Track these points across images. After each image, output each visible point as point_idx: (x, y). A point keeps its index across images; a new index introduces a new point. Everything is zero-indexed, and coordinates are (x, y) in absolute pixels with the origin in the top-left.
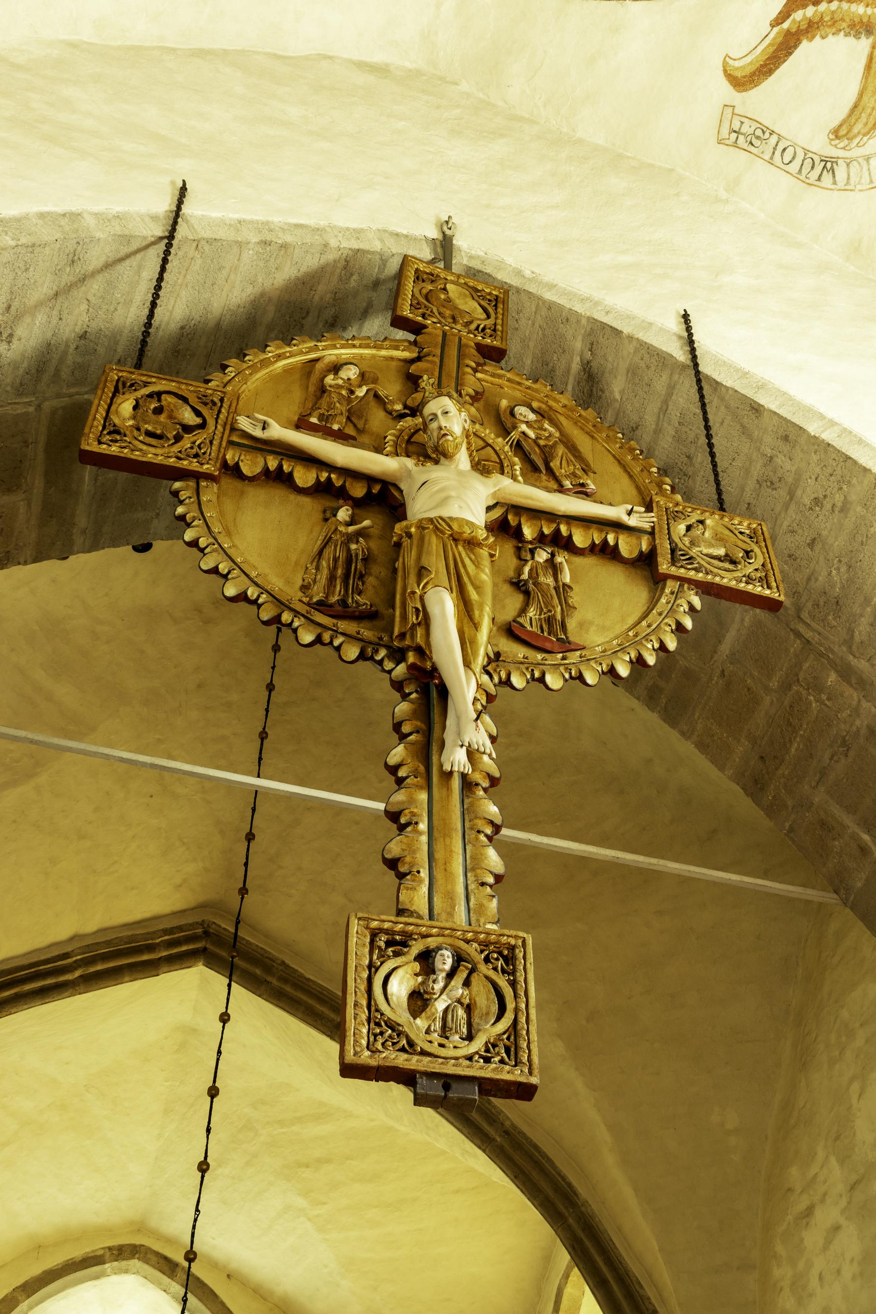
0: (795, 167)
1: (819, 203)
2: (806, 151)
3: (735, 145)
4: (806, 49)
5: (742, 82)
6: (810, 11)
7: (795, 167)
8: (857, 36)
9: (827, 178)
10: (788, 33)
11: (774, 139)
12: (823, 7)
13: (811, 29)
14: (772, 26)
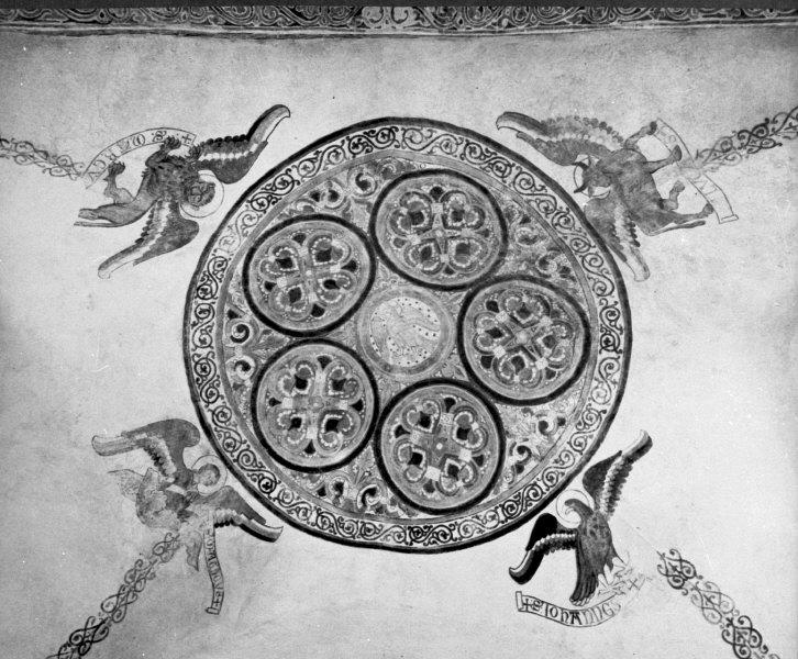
0: (558, 618)
1: (573, 633)
2: (562, 609)
3: (527, 611)
4: (547, 559)
5: (522, 578)
6: (543, 540)
7: (558, 618)
8: (568, 548)
9: (576, 621)
10: (535, 551)
11: (545, 605)
12: (548, 538)
13: (546, 549)
14: (528, 549)
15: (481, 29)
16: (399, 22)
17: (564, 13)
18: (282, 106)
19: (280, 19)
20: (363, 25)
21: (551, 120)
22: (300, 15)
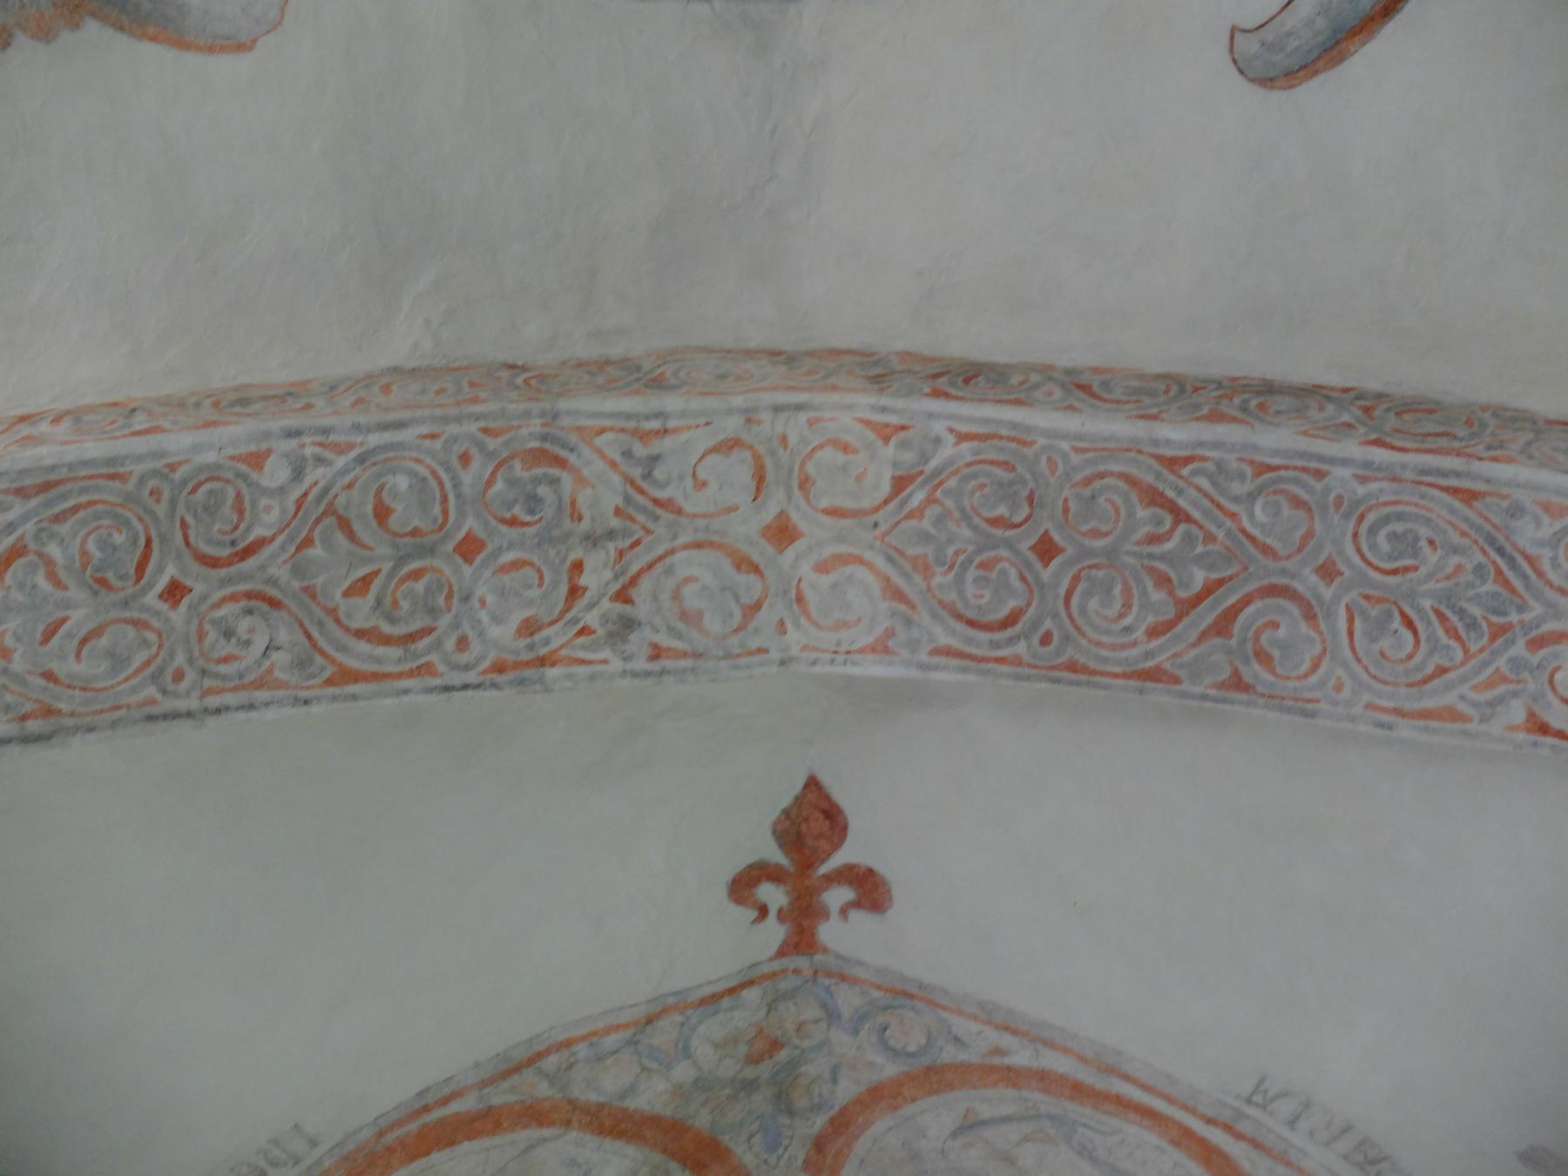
15: (374, 439)
16: (729, 446)
17: (30, 527)
18: (1267, 82)
19: (1238, 488)
20: (886, 433)
21: (45, 34)
22: (1154, 498)
